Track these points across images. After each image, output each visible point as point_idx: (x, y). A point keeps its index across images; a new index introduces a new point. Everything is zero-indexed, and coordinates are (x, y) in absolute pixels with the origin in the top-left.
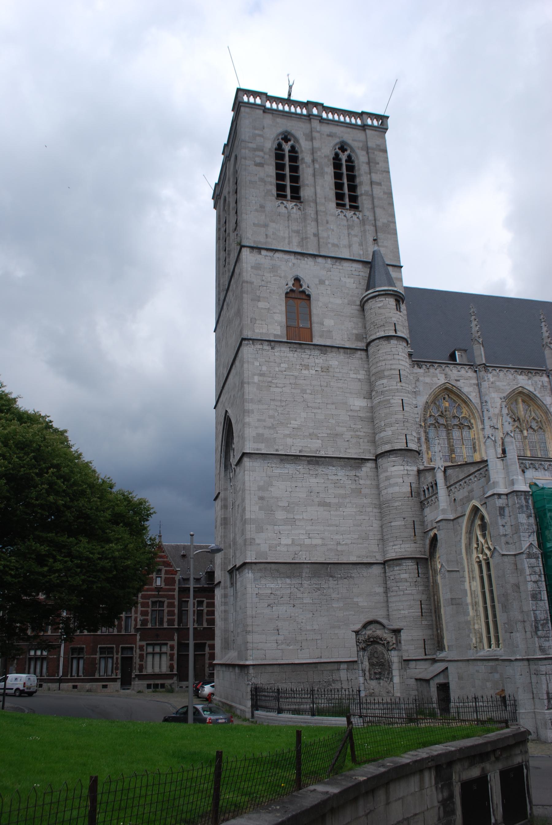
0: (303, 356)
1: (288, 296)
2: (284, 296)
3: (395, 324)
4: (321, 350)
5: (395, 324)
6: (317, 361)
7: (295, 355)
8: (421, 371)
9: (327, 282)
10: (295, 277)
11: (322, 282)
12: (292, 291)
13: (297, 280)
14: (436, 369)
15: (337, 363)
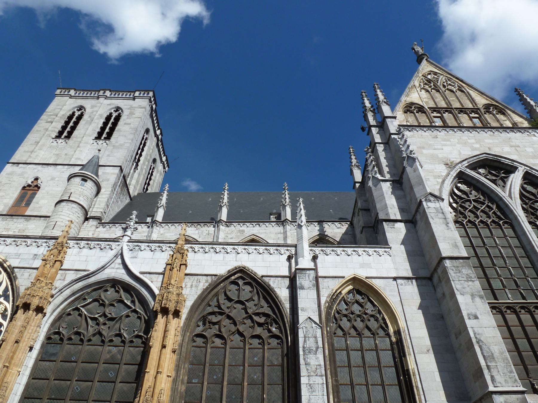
0: (10, 223)
1: (25, 189)
2: (21, 188)
3: (71, 193)
4: (26, 219)
5: (71, 193)
6: (18, 226)
7: (4, 223)
8: (105, 229)
9: (57, 179)
10: (35, 178)
11: (53, 179)
12: (29, 186)
13: (36, 179)
14: (116, 228)
15: (34, 226)
